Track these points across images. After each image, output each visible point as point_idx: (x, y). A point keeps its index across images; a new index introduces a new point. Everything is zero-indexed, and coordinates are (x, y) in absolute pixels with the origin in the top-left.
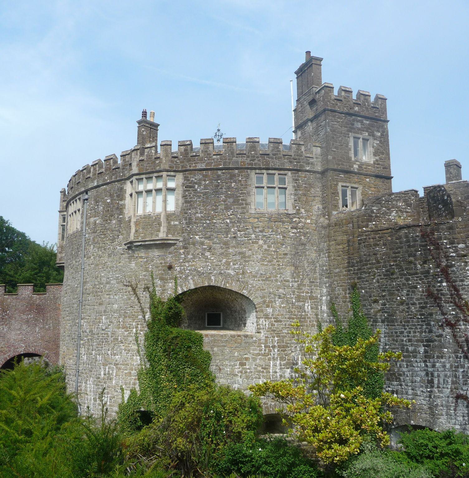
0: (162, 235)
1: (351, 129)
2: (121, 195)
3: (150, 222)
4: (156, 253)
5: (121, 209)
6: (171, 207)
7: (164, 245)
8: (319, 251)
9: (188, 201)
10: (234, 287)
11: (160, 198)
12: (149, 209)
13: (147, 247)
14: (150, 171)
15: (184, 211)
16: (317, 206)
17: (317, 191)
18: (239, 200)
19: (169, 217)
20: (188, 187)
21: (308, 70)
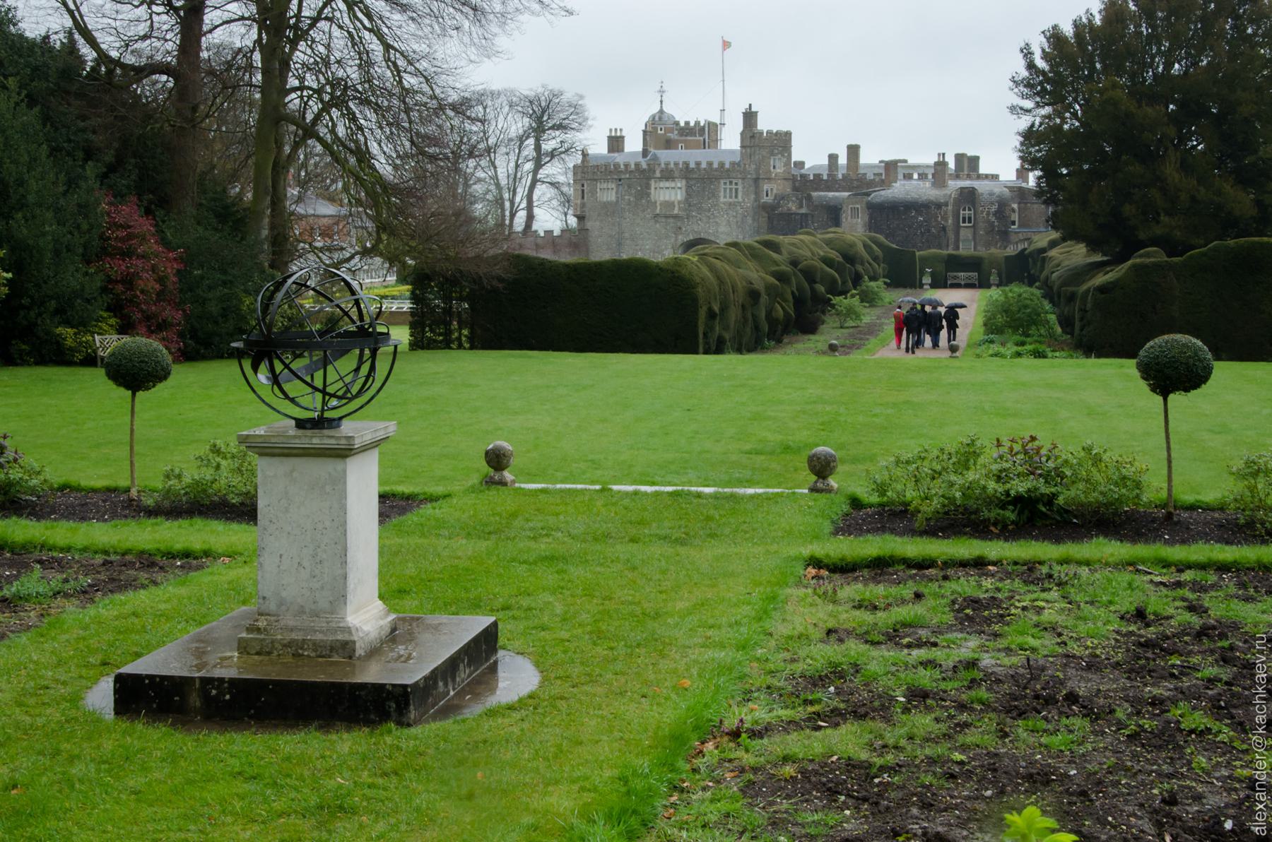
0: (676, 211)
1: (772, 154)
2: (648, 186)
3: (669, 204)
4: (671, 220)
5: (648, 195)
6: (679, 197)
7: (676, 217)
8: (754, 220)
9: (689, 195)
10: (712, 238)
11: (673, 192)
12: (667, 198)
13: (666, 217)
14: (668, 175)
15: (686, 199)
16: (753, 196)
17: (752, 189)
18: (714, 195)
19: (679, 202)
20: (688, 187)
21: (750, 117)
